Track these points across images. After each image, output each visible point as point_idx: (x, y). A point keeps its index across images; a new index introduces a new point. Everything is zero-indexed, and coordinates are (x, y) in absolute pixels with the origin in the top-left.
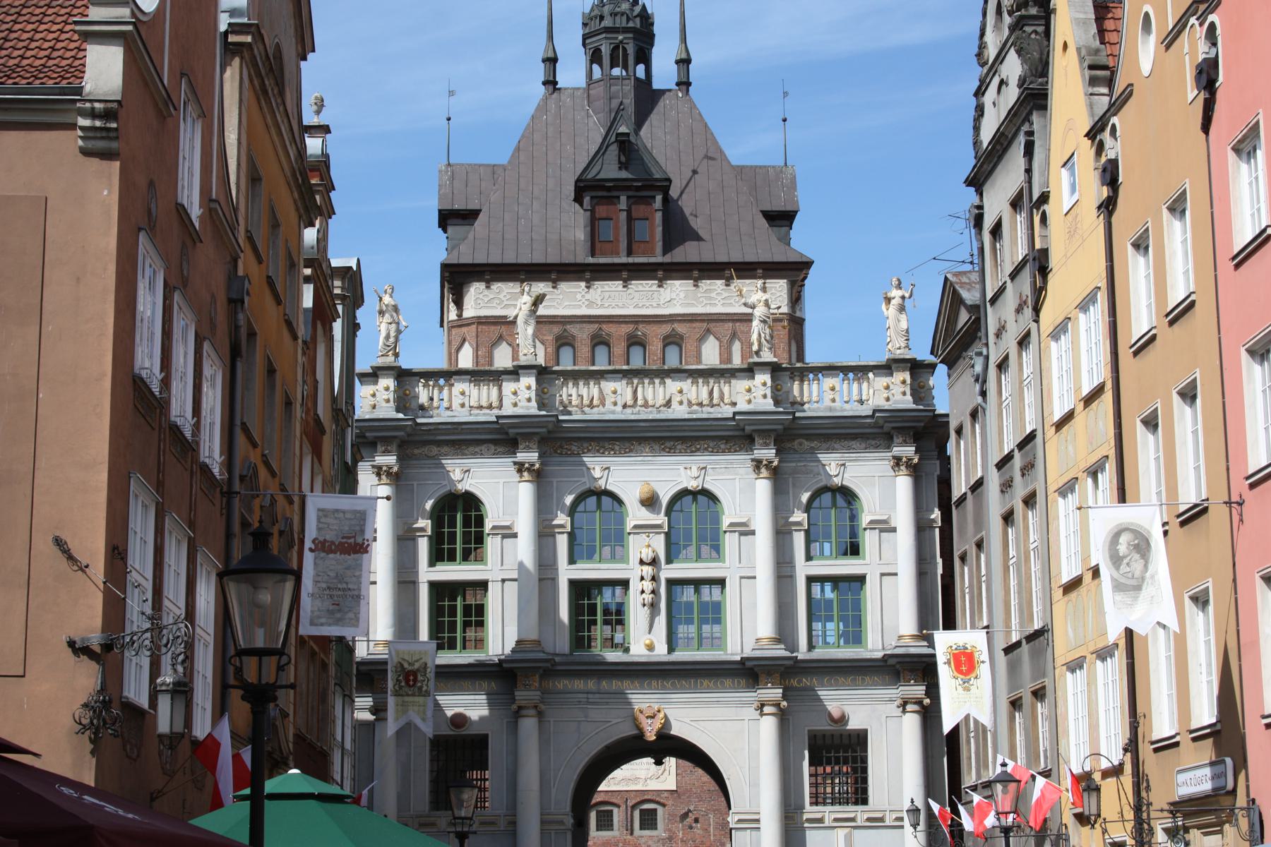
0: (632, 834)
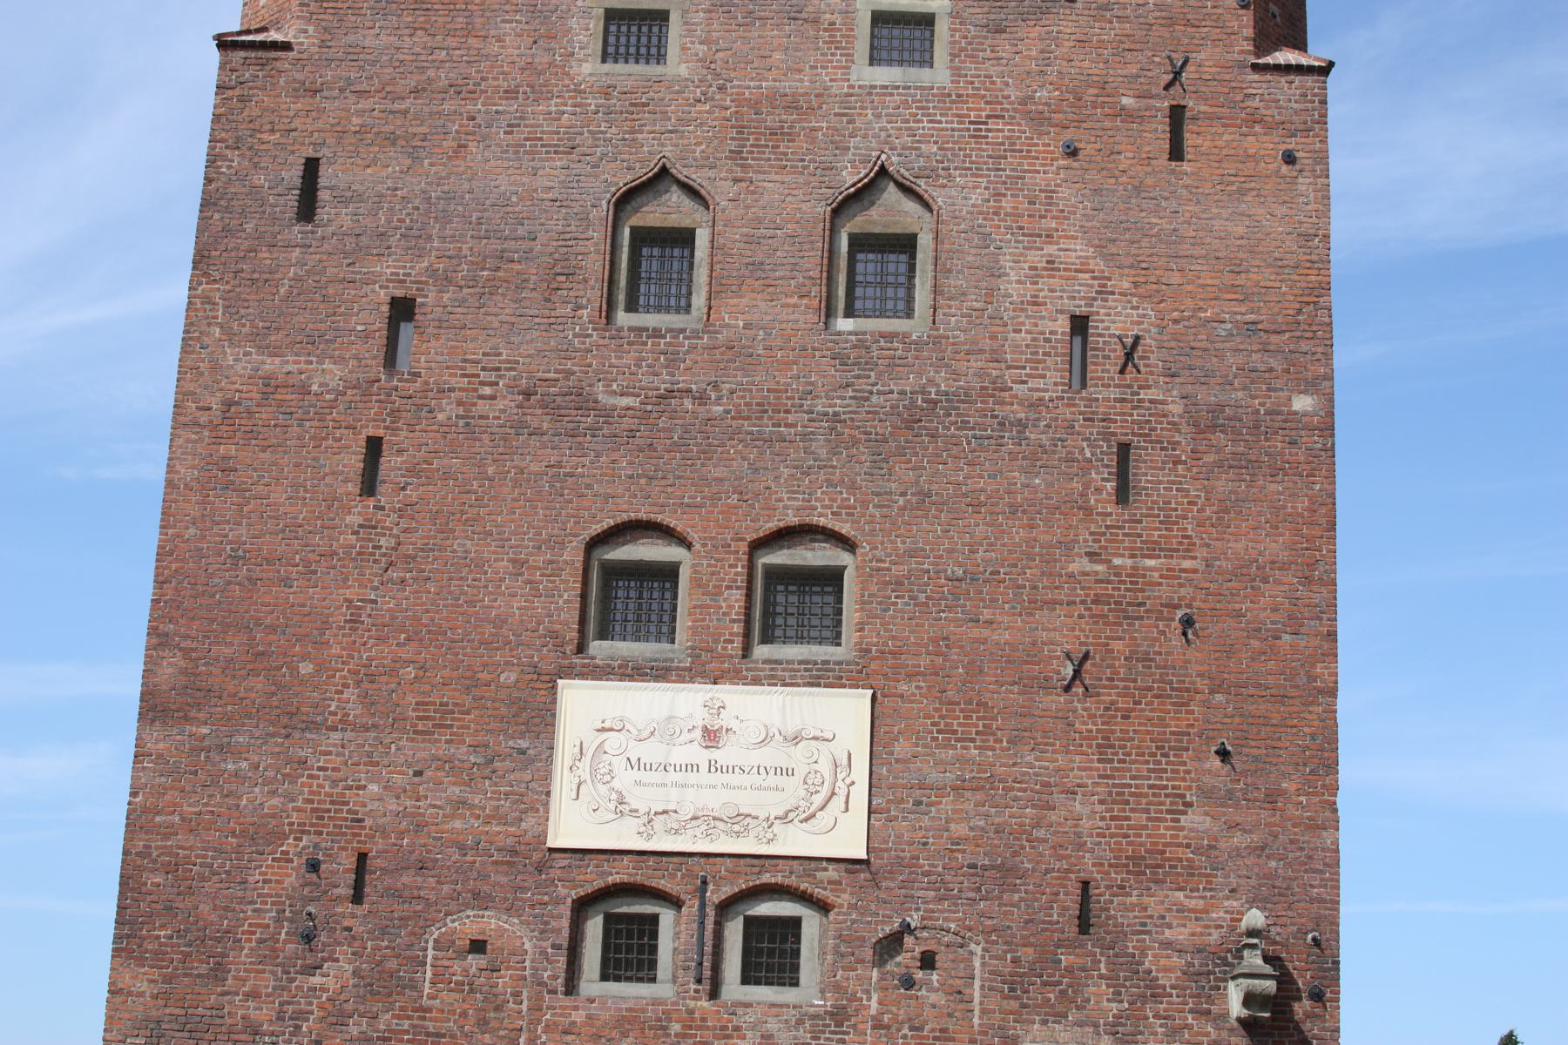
0: (714, 994)
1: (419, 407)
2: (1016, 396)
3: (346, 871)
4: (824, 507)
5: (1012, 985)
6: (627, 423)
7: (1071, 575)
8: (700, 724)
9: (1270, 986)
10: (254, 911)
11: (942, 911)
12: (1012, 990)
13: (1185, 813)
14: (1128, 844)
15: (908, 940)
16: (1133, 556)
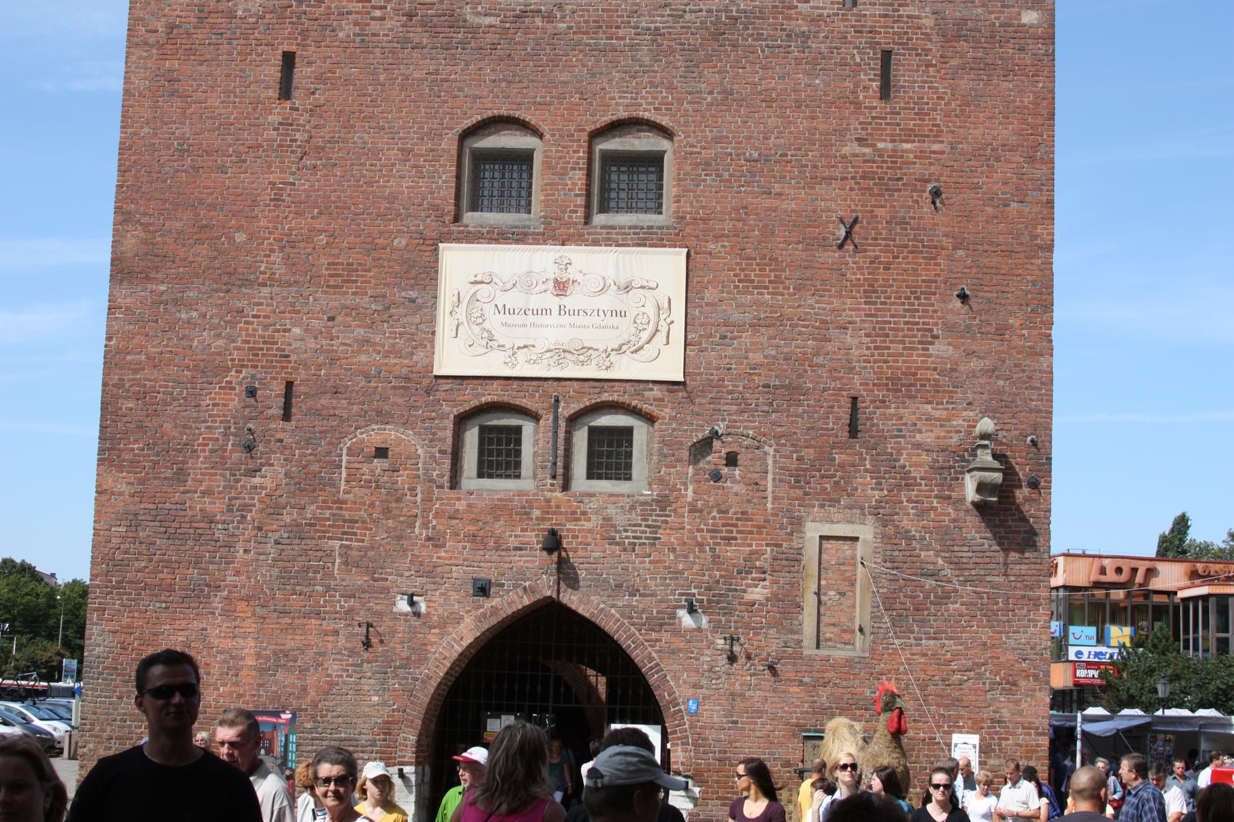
0: (566, 487)
1: (324, 27)
2: (800, 13)
3: (277, 396)
4: (648, 104)
5: (797, 478)
6: (490, 38)
7: (844, 157)
8: (552, 277)
9: (997, 477)
10: (207, 428)
11: (742, 421)
12: (797, 481)
13: (932, 343)
14: (888, 368)
15: (716, 444)
16: (893, 141)
